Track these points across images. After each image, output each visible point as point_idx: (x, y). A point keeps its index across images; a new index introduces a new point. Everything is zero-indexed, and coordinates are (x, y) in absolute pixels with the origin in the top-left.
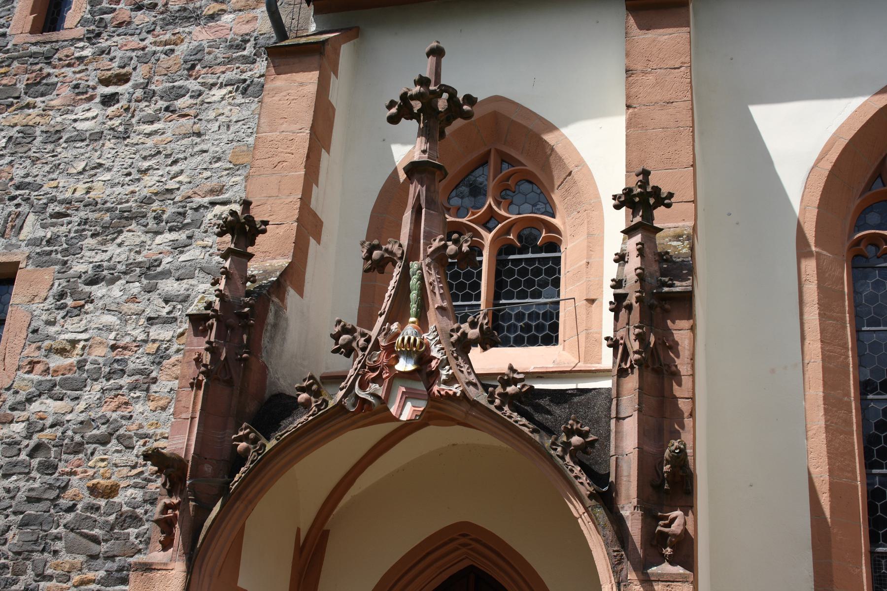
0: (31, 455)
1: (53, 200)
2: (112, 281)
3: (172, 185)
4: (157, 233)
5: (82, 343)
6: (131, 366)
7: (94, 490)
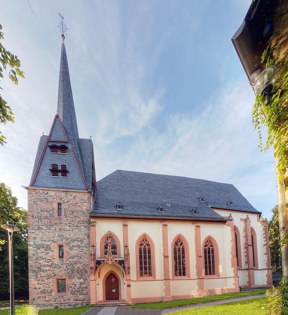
1: (66, 237)
2: (75, 247)
6: (79, 256)
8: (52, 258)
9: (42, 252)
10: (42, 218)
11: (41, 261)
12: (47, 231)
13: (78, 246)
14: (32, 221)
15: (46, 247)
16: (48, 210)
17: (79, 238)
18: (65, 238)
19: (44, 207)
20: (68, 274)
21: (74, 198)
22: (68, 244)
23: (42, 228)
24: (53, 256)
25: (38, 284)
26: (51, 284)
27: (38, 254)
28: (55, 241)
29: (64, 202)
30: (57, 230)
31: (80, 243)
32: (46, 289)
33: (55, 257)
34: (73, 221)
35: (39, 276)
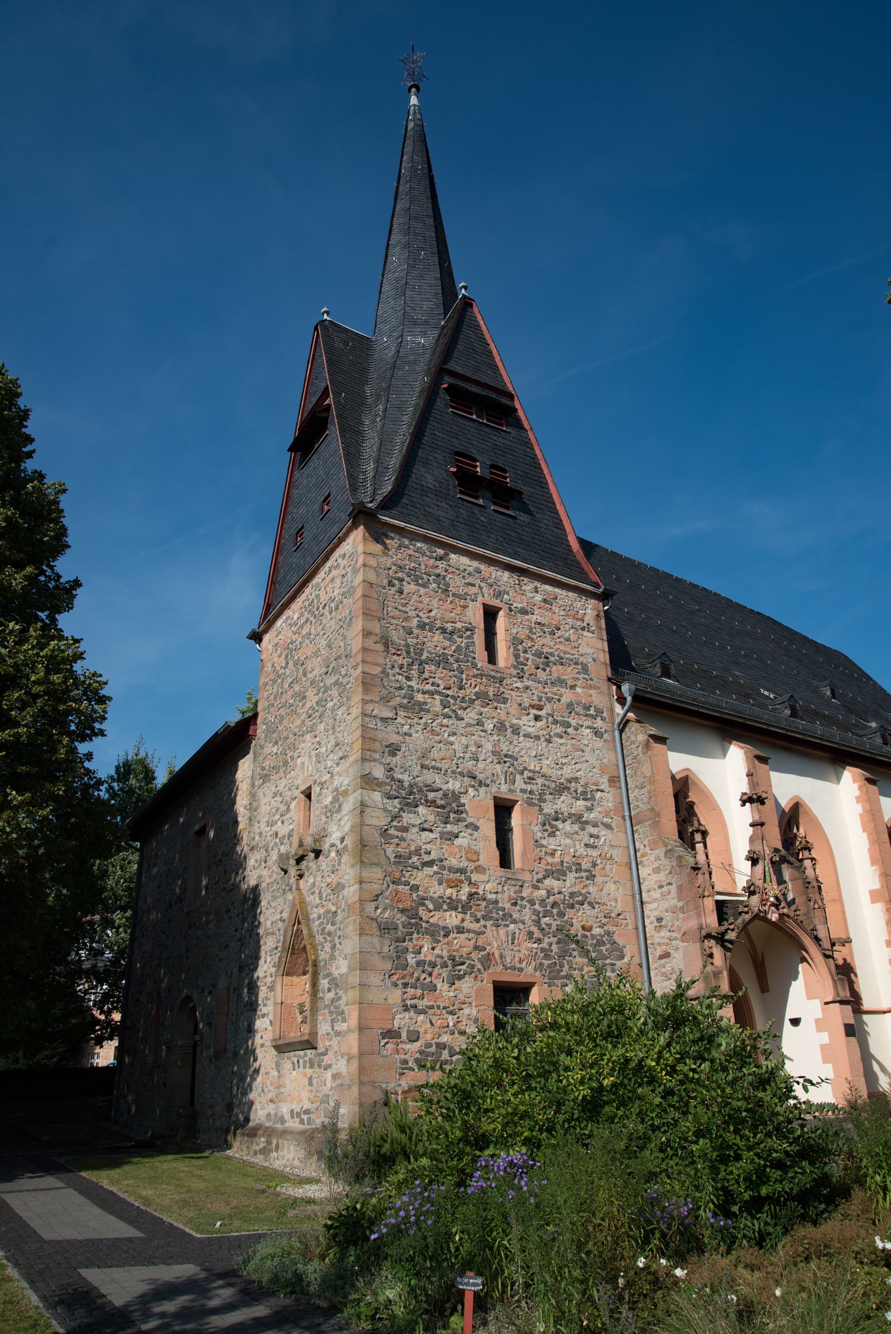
0: (552, 907)
2: (564, 821)
3: (578, 774)
4: (578, 799)
5: (559, 852)
7: (583, 928)
8: (472, 865)
9: (425, 826)
10: (424, 657)
11: (420, 874)
12: (445, 721)
13: (578, 818)
14: (381, 660)
15: (443, 802)
16: (449, 626)
17: (576, 779)
18: (522, 773)
19: (430, 611)
20: (547, 957)
21: (545, 601)
22: (535, 801)
23: (425, 703)
24: (477, 853)
25: (406, 1008)
26: (467, 1011)
27: (404, 835)
28: (481, 777)
29: (511, 610)
30: (489, 726)
31: (581, 803)
32: (445, 1038)
33: (483, 861)
34: (549, 700)
35: (411, 959)
